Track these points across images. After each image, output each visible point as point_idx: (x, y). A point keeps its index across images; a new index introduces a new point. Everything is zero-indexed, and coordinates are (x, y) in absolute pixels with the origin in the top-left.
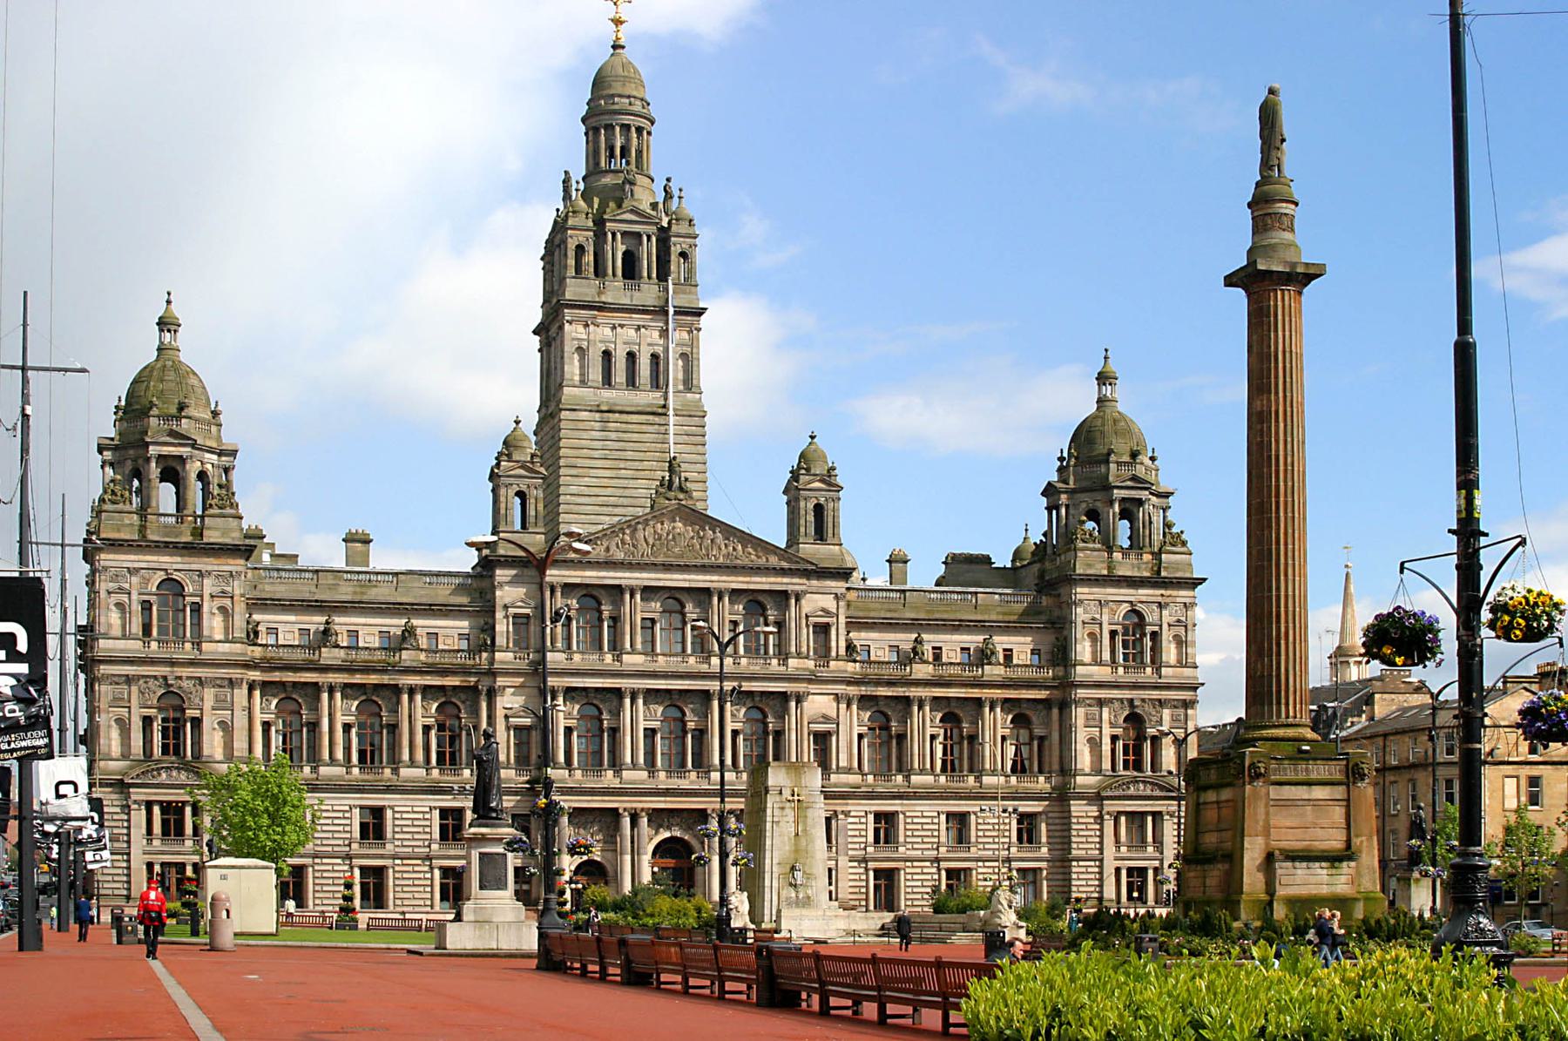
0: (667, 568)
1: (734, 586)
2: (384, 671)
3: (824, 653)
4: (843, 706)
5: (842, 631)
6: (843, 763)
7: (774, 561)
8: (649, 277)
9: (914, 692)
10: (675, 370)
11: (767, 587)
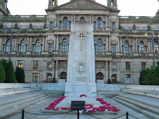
0: (81, 10)
1: (95, 14)
2: (24, 33)
5: (118, 23)
7: (103, 8)
9: (134, 36)
11: (101, 14)
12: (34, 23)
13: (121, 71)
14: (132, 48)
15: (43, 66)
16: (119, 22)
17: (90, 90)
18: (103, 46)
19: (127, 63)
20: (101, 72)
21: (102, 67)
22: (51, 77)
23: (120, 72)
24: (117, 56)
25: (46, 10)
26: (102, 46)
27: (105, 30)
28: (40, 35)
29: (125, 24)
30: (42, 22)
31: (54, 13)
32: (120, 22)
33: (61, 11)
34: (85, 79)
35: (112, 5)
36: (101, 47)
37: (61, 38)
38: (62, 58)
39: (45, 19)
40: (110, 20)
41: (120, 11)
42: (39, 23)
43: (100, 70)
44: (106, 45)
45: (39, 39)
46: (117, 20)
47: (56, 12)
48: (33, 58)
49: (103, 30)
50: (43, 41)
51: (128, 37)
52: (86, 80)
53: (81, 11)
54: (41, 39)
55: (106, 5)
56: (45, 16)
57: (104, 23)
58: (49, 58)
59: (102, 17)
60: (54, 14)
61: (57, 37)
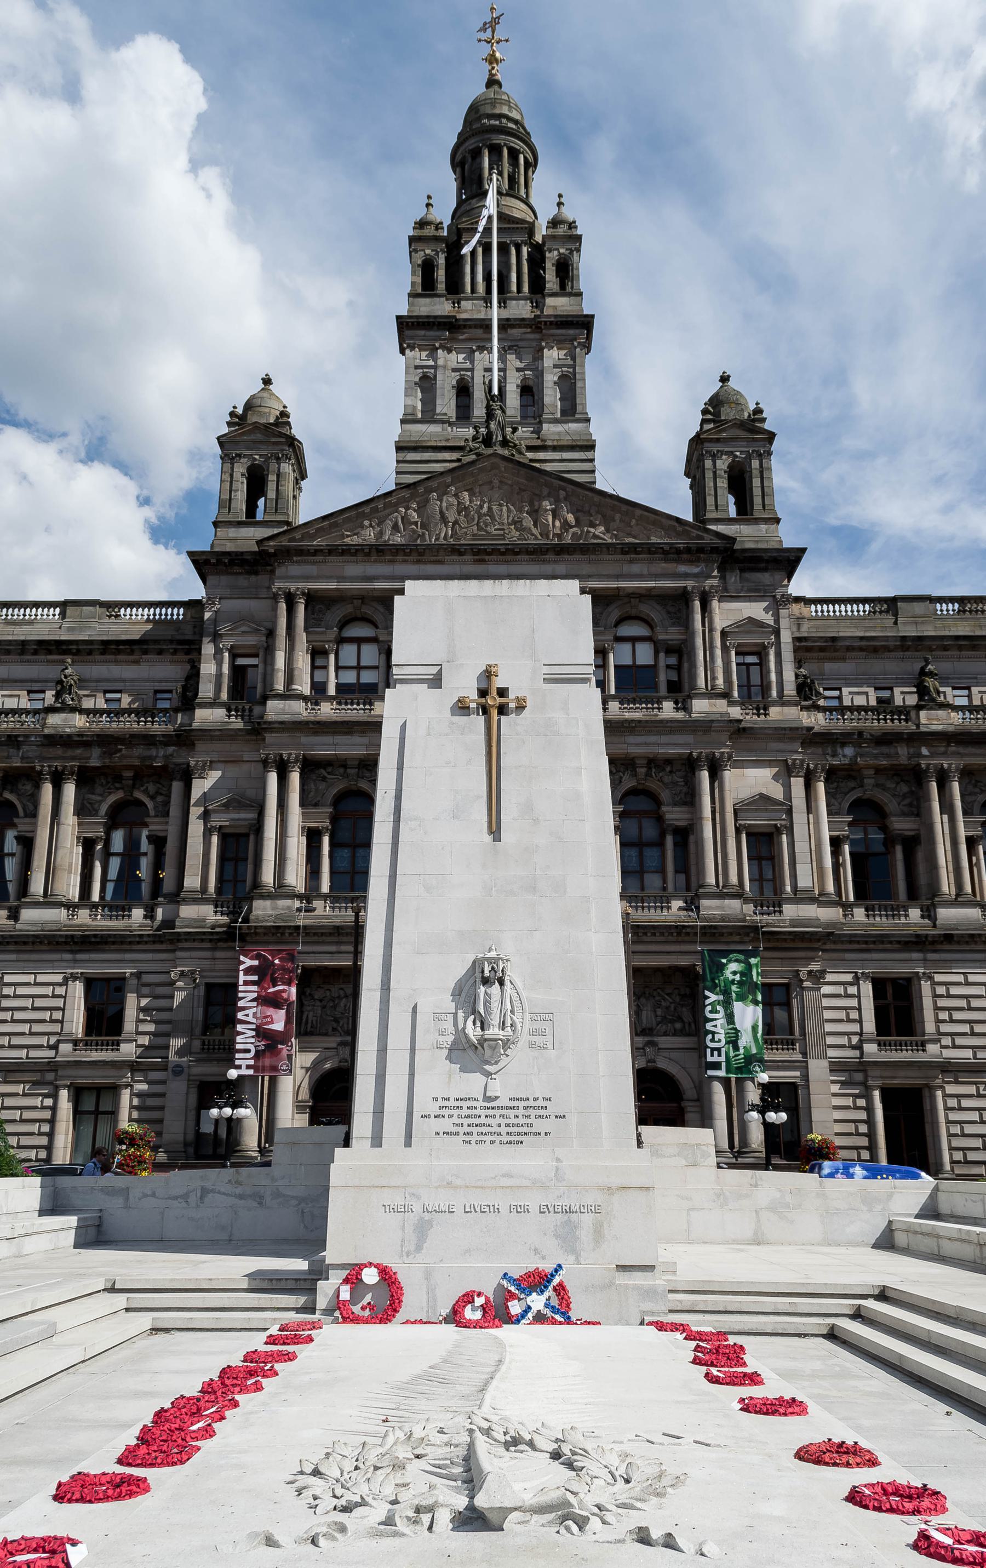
3: (756, 693)
4: (798, 784)
6: (805, 881)
8: (519, 289)
10: (552, 397)
12: (95, 662)
13: (831, 1053)
14: (920, 856)
15: (168, 1022)
16: (796, 650)
17: (585, 1236)
18: (669, 840)
19: (879, 985)
20: (662, 1064)
21: (664, 1020)
22: (228, 1111)
23: (825, 1063)
24: (794, 923)
25: (196, 563)
26: (661, 844)
27: (680, 715)
28: (143, 758)
29: (843, 659)
30: (160, 652)
31: (262, 579)
32: (808, 649)
33: (314, 563)
34: (520, 1123)
35: (732, 512)
36: (651, 854)
37: (322, 786)
38: (333, 948)
39: (188, 634)
40: (724, 634)
41: (797, 561)
42: (137, 662)
43: (651, 1044)
44: (692, 839)
45: (138, 795)
46: (777, 632)
47: (280, 571)
48: (79, 956)
49: (668, 710)
50: (167, 814)
51: (878, 771)
52: (540, 1125)
53: (482, 561)
54: (152, 798)
55: (689, 517)
56: (193, 605)
57: (673, 660)
58: (219, 954)
59: (658, 607)
60: (263, 593)
61: (295, 778)
